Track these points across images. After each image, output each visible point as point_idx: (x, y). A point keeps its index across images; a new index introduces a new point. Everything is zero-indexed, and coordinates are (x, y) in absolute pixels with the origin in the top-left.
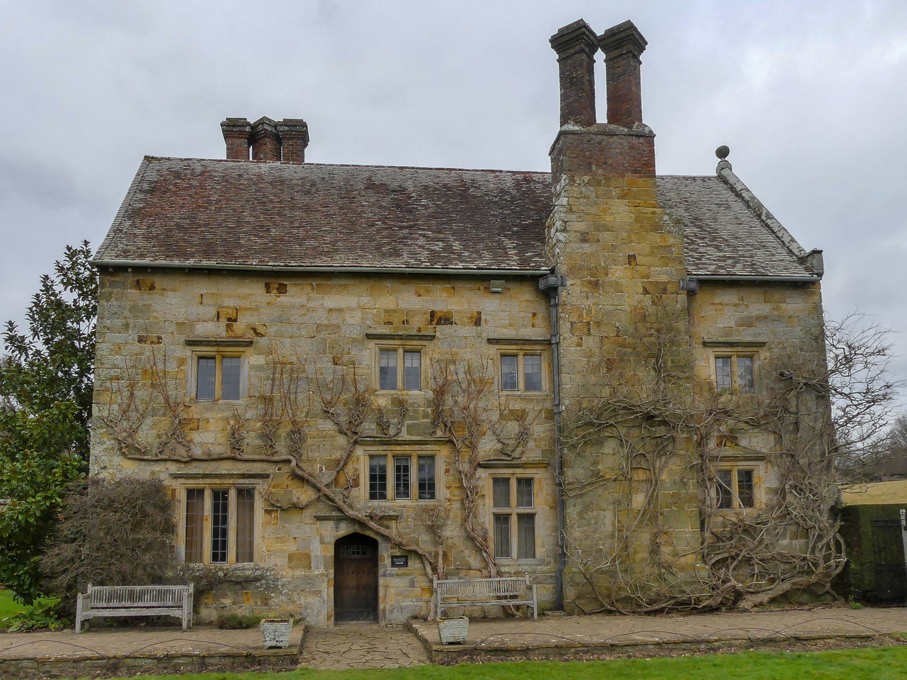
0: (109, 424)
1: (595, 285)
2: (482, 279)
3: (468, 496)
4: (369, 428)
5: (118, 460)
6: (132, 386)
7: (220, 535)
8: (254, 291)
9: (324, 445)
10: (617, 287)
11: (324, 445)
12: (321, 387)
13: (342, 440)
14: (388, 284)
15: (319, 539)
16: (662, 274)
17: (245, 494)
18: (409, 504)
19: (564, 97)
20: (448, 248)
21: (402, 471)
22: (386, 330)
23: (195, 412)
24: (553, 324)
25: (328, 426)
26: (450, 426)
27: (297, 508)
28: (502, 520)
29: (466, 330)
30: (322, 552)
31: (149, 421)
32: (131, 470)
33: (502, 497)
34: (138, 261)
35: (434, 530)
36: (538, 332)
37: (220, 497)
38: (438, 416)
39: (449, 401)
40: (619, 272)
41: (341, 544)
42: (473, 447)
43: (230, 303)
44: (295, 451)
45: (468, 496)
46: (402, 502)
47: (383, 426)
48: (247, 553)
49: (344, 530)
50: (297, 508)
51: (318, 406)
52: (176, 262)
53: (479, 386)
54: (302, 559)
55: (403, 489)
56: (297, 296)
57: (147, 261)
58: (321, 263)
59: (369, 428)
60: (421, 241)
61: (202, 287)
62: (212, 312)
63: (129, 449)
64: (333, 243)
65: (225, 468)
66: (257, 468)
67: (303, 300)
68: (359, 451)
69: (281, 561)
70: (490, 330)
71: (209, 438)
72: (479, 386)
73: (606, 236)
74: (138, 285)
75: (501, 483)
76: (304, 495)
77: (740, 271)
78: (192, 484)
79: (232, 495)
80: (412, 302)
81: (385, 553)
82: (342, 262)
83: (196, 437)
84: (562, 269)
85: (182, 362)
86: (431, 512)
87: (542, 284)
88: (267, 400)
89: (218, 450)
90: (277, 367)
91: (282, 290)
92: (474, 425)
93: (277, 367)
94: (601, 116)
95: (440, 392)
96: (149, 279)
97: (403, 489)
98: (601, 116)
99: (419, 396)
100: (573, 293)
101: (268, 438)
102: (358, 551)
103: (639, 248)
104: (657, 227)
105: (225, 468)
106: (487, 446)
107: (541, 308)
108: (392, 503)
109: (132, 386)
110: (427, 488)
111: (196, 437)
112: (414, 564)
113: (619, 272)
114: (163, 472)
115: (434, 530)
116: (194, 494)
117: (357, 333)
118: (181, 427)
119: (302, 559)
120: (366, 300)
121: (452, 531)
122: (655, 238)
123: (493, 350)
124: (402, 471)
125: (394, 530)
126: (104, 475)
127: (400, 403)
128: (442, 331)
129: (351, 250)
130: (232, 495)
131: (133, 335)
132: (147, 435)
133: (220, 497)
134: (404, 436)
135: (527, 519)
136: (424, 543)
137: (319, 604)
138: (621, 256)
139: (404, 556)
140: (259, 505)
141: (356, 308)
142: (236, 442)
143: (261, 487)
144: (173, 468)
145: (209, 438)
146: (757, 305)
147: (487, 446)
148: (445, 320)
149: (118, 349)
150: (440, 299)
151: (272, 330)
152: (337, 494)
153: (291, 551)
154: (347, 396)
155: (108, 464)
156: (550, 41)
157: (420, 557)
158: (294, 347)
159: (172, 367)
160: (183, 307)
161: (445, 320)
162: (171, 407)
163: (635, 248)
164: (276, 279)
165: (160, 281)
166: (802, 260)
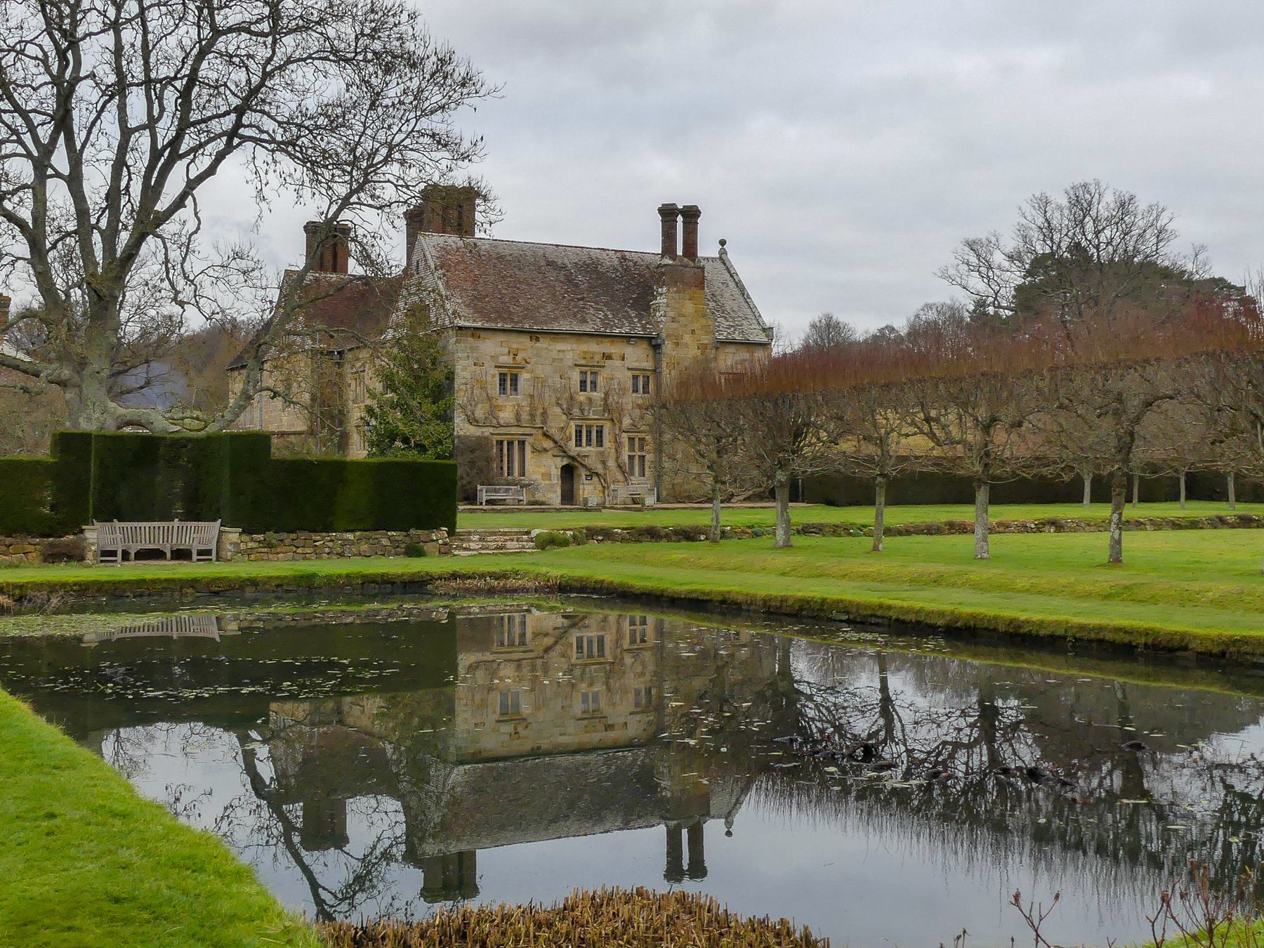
0: (463, 407)
1: (677, 344)
2: (627, 338)
3: (618, 446)
4: (576, 411)
5: (467, 425)
6: (472, 389)
7: (510, 462)
8: (525, 341)
9: (557, 420)
10: (687, 345)
11: (557, 420)
12: (555, 390)
13: (564, 417)
14: (584, 338)
15: (554, 465)
16: (706, 339)
17: (522, 443)
18: (591, 450)
19: (663, 242)
20: (606, 315)
21: (589, 433)
22: (583, 362)
23: (500, 402)
24: (658, 363)
25: (558, 410)
26: (611, 411)
27: (546, 450)
28: (631, 458)
29: (618, 363)
30: (556, 472)
31: (480, 406)
32: (472, 431)
33: (632, 448)
34: (475, 325)
35: (604, 462)
36: (648, 365)
37: (510, 443)
38: (606, 407)
39: (611, 399)
40: (687, 338)
41: (563, 468)
42: (620, 422)
43: (515, 346)
44: (544, 422)
45: (618, 446)
46: (589, 448)
47: (582, 411)
48: (523, 473)
49: (565, 462)
50: (546, 450)
51: (554, 400)
52: (493, 326)
53: (623, 391)
54: (547, 476)
55: (589, 443)
56: (543, 343)
57: (479, 325)
58: (556, 327)
59: (576, 411)
60: (592, 311)
61: (501, 338)
62: (506, 350)
63: (472, 420)
64: (553, 311)
65: (514, 430)
66: (527, 431)
67: (545, 346)
68: (572, 423)
69: (539, 477)
71: (506, 415)
72: (623, 391)
73: (682, 319)
74: (473, 336)
75: (631, 439)
77: (738, 337)
78: (499, 438)
79: (516, 443)
80: (594, 347)
81: (583, 473)
82: (564, 326)
83: (501, 415)
84: (663, 335)
85: (494, 376)
86: (602, 453)
87: (654, 342)
88: (532, 396)
89: (513, 421)
90: (536, 378)
91: (537, 340)
92: (621, 410)
93: (536, 378)
94: (680, 252)
95: (607, 394)
96: (478, 333)
97: (589, 443)
98: (680, 252)
99: (597, 395)
100: (668, 348)
101: (532, 416)
102: (568, 473)
104: (704, 316)
105: (514, 430)
106: (627, 422)
107: (651, 353)
108: (585, 449)
109: (472, 389)
110: (600, 442)
111: (501, 415)
112: (595, 479)
113: (687, 338)
115: (604, 462)
117: (570, 363)
118: (493, 410)
119: (547, 476)
120: (574, 346)
121: (611, 463)
122: (703, 321)
123: (630, 374)
124: (589, 433)
125: (587, 462)
126: (461, 433)
127: (590, 399)
128: (608, 362)
129: (564, 317)
130: (516, 443)
131: (471, 362)
132: (480, 413)
133: (510, 443)
134: (591, 416)
135: (642, 458)
136: (600, 470)
137: (555, 498)
138: (689, 329)
139: (592, 474)
140: (528, 449)
141: (570, 351)
142: (518, 417)
143: (529, 440)
144: (491, 430)
145: (506, 415)
148: (608, 357)
149: (465, 369)
151: (533, 361)
153: (543, 470)
154: (567, 395)
155: (461, 427)
156: (660, 210)
157: (597, 474)
158: (543, 370)
159: (489, 379)
160: (494, 349)
161: (608, 357)
162: (489, 399)
163: (696, 326)
164: (534, 335)
165: (482, 334)
166: (764, 330)
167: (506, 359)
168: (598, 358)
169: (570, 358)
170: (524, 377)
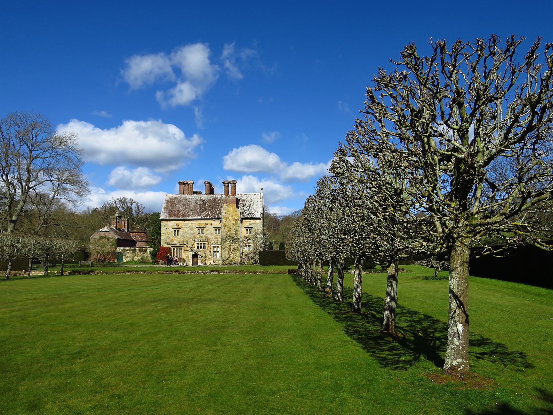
2: (211, 219)
15: (190, 255)
17: (181, 249)
29: (210, 226)
30: (190, 256)
32: (166, 246)
40: (230, 218)
41: (193, 255)
56: (187, 222)
58: (190, 217)
70: (213, 226)
76: (188, 249)
82: (193, 217)
100: (224, 221)
102: (195, 256)
103: (233, 215)
113: (230, 218)
114: (170, 246)
116: (174, 249)
117: (195, 227)
133: (177, 249)
136: (204, 255)
146: (252, 221)
147: (212, 242)
150: (206, 222)
152: (192, 249)
155: (163, 244)
158: (187, 229)
160: (172, 224)
163: (233, 215)
167: (176, 227)
168: (203, 225)
169: (194, 226)
170: (181, 231)
